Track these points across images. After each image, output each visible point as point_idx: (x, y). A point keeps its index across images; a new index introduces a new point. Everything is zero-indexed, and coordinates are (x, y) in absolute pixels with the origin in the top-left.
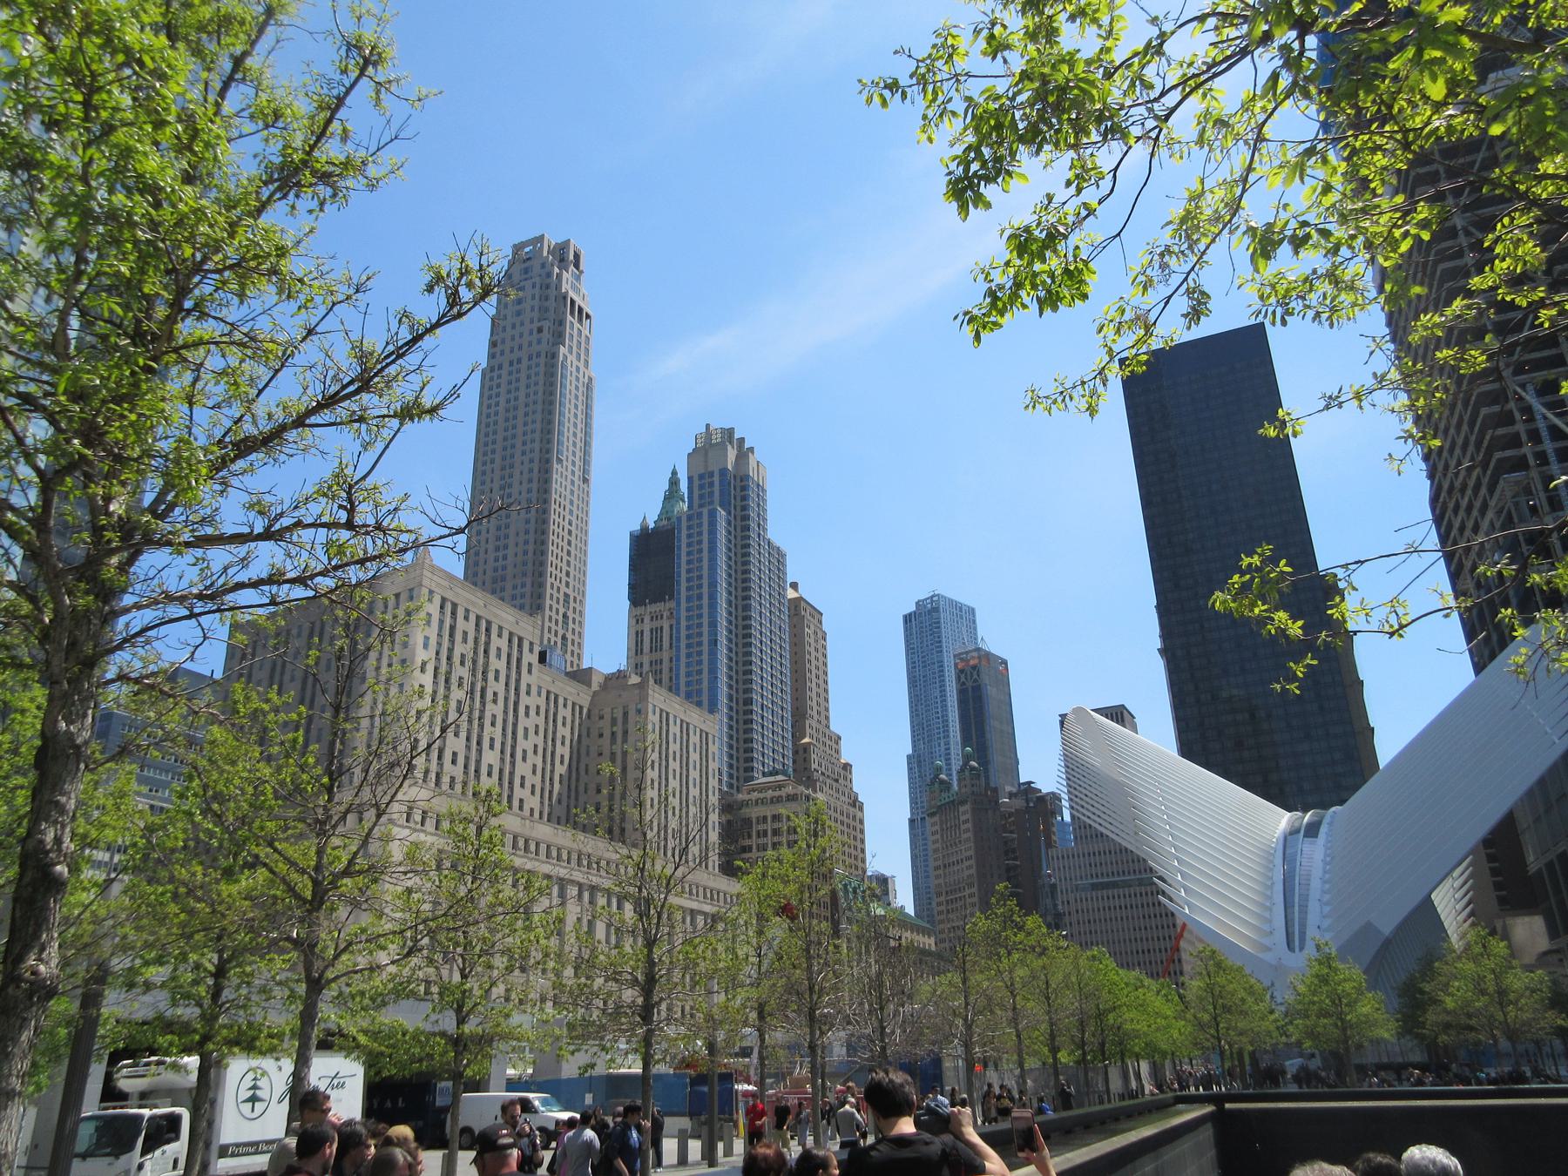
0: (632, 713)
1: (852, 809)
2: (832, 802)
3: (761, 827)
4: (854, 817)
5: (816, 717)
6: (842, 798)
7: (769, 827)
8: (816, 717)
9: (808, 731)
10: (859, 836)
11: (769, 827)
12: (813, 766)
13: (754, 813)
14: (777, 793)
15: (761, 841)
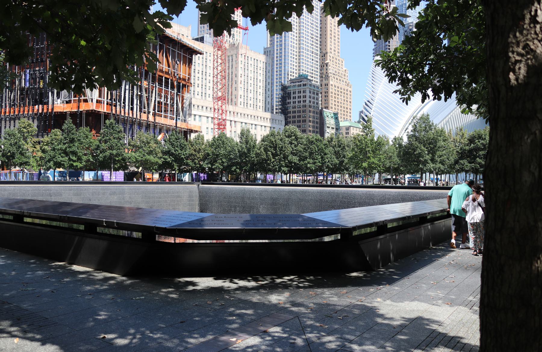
0: (234, 58)
1: (346, 88)
2: (337, 85)
3: (294, 95)
4: (347, 90)
5: (333, 52)
6: (342, 83)
7: (297, 95)
8: (333, 52)
9: (328, 58)
10: (349, 97)
11: (297, 95)
12: (329, 71)
13: (291, 90)
14: (300, 83)
15: (295, 100)
